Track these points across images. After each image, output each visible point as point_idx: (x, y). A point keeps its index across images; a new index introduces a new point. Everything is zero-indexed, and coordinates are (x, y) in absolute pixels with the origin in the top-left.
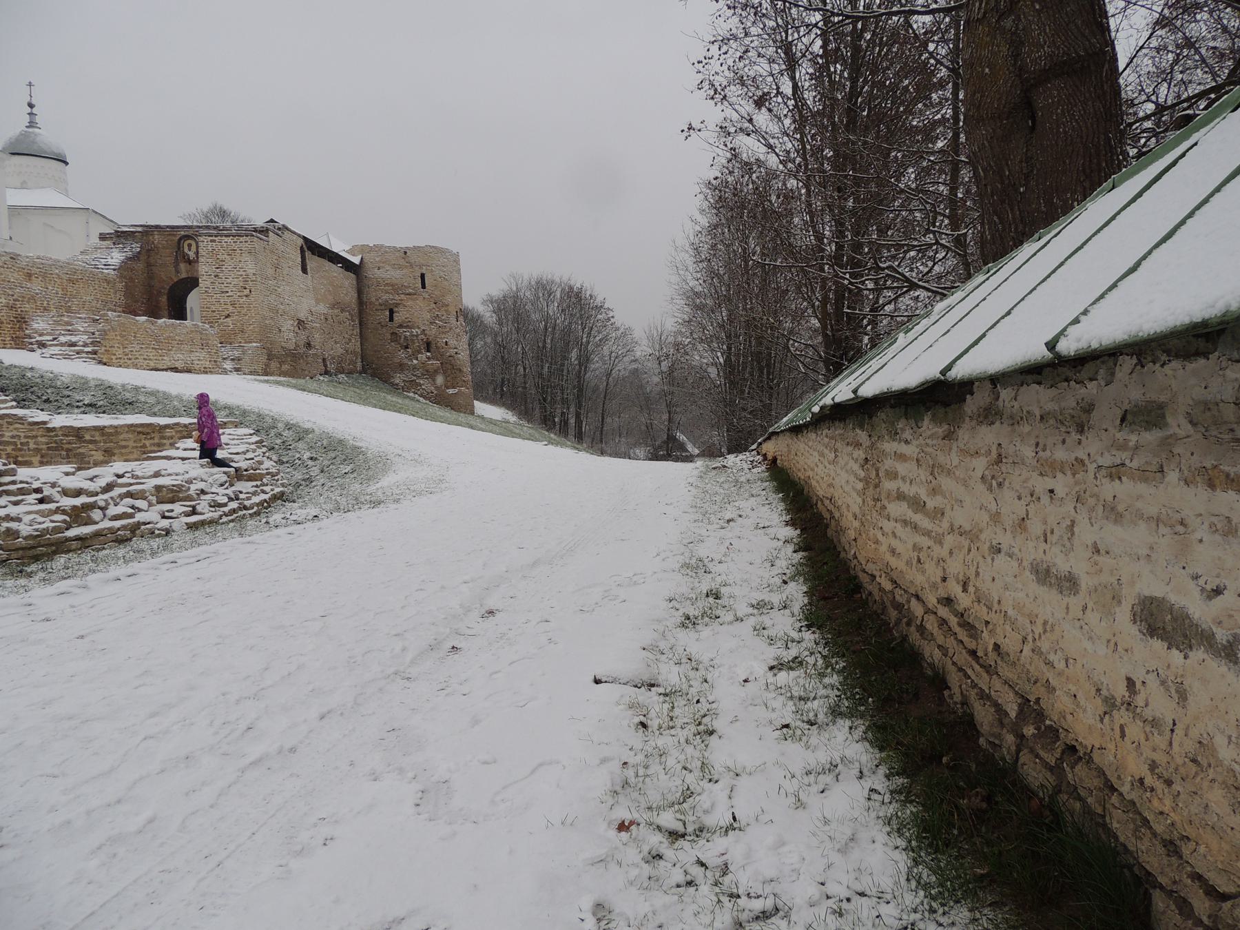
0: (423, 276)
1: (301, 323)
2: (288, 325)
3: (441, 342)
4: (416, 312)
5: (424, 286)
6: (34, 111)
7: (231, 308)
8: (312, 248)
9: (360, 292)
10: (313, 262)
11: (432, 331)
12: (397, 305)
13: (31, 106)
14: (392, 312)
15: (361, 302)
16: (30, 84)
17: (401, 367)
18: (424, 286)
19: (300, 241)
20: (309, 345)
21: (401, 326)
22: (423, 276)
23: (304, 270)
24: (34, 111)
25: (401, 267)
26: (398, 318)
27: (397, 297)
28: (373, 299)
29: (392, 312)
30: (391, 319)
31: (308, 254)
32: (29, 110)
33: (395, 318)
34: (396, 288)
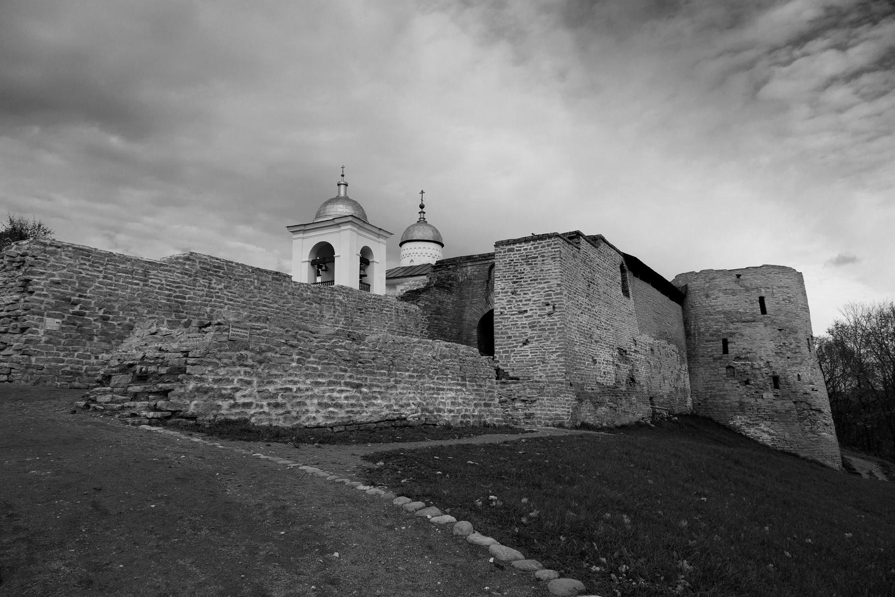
0: (762, 300)
1: (622, 352)
2: (605, 355)
3: (792, 378)
4: (759, 344)
5: (764, 311)
6: (424, 210)
7: (529, 332)
8: (634, 267)
9: (686, 323)
10: (637, 285)
11: (779, 365)
12: (732, 334)
13: (422, 207)
14: (725, 343)
15: (688, 334)
16: (422, 192)
17: (742, 407)
18: (764, 311)
19: (620, 259)
20: (632, 380)
21: (738, 358)
22: (762, 300)
23: (626, 293)
24: (424, 210)
25: (734, 293)
27: (731, 326)
28: (702, 330)
30: (726, 351)
31: (629, 275)
32: (420, 210)
33: (730, 350)
34: (730, 317)
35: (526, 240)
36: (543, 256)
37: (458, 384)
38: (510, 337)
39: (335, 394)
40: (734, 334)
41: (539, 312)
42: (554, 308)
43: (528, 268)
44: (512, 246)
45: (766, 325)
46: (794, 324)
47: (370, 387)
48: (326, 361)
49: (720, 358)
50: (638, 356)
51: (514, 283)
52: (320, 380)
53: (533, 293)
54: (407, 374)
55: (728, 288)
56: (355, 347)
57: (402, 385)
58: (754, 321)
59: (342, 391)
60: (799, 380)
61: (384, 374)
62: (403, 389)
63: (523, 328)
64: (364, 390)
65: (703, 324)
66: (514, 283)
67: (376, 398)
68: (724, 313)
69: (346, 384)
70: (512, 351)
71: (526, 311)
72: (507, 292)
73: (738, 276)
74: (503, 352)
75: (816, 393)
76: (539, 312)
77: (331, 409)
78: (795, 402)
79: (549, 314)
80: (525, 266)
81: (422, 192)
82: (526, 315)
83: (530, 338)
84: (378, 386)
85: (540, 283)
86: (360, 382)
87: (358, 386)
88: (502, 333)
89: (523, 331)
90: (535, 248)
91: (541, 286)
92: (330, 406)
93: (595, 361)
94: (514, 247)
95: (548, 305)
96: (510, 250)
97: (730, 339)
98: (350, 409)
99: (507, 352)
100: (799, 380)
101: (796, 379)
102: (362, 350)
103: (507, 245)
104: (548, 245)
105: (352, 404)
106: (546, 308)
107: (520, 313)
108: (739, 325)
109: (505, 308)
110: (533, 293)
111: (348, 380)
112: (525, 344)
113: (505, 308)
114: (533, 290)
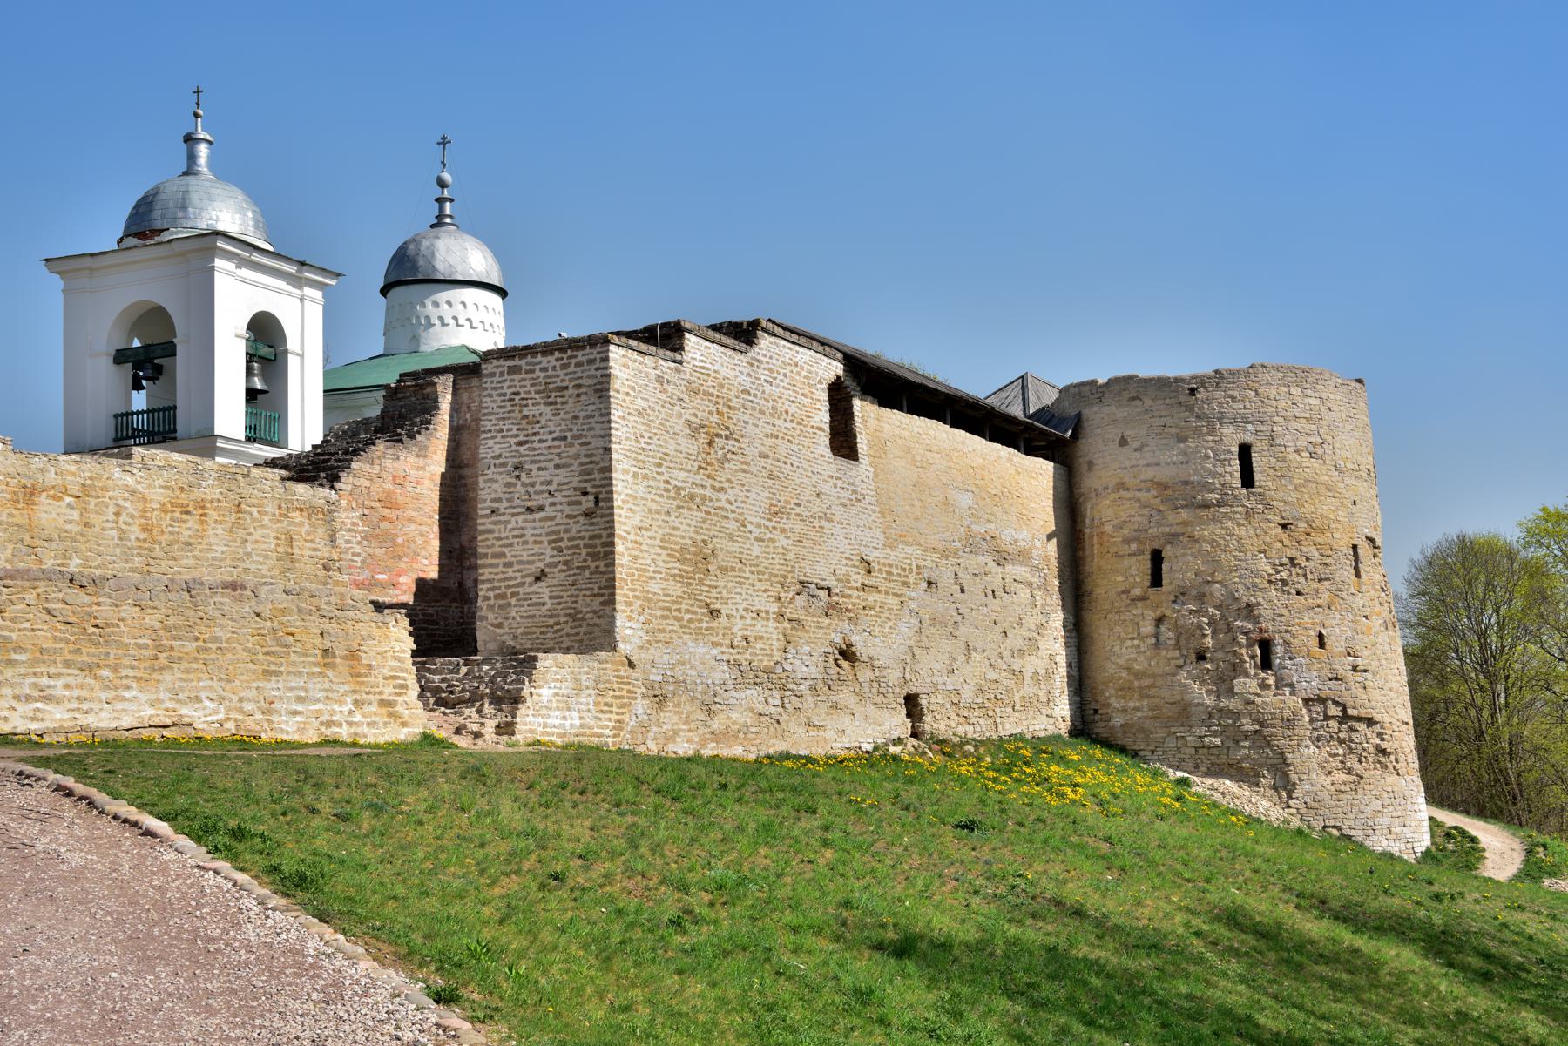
0: (1245, 451)
5: (1248, 479)
12: (1173, 538)
14: (1157, 558)
16: (444, 142)
18: (1248, 479)
19: (836, 368)
22: (1245, 451)
26: (1177, 572)
27: (1171, 517)
28: (1108, 528)
29: (1157, 558)
30: (1156, 580)
32: (437, 192)
35: (547, 349)
36: (579, 386)
37: (316, 664)
38: (509, 565)
39: (45, 681)
40: (1176, 535)
41: (568, 511)
42: (597, 500)
43: (547, 410)
44: (517, 362)
45: (1249, 514)
46: (1324, 509)
47: (115, 668)
48: (27, 625)
49: (1143, 599)
50: (872, 598)
51: (520, 444)
52: (17, 657)
53: (557, 466)
54: (195, 644)
55: (1168, 421)
56: (87, 599)
57: (185, 665)
58: (1221, 504)
59: (59, 675)
60: (1322, 645)
61: (146, 647)
62: (187, 671)
63: (535, 542)
64: (104, 673)
65: (1110, 512)
66: (520, 444)
67: (128, 688)
68: (1159, 484)
69: (67, 664)
70: (513, 595)
71: (541, 508)
72: (504, 465)
73: (1193, 391)
74: (496, 597)
75: (1359, 677)
76: (568, 511)
77: (39, 705)
78: (1306, 701)
79: (586, 515)
80: (542, 407)
81: (444, 142)
82: (542, 514)
83: (550, 565)
84: (132, 668)
85: (571, 445)
86: (95, 660)
87: (88, 669)
88: (495, 556)
89: (537, 549)
90: (565, 366)
91: (572, 451)
92: (36, 700)
93: (714, 613)
94: (523, 362)
95: (585, 494)
96: (514, 370)
97: (1168, 552)
98: (75, 705)
99: (502, 596)
100: (1322, 645)
101: (1315, 642)
102: (98, 604)
103: (507, 358)
104: (590, 362)
105: (78, 698)
106: (583, 499)
107: (530, 510)
108: (1184, 515)
109: (499, 500)
110: (557, 466)
111: (69, 657)
112: (538, 579)
113: (499, 500)
114: (557, 461)
